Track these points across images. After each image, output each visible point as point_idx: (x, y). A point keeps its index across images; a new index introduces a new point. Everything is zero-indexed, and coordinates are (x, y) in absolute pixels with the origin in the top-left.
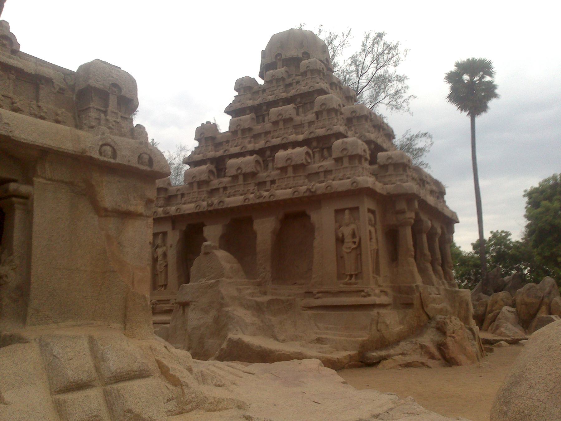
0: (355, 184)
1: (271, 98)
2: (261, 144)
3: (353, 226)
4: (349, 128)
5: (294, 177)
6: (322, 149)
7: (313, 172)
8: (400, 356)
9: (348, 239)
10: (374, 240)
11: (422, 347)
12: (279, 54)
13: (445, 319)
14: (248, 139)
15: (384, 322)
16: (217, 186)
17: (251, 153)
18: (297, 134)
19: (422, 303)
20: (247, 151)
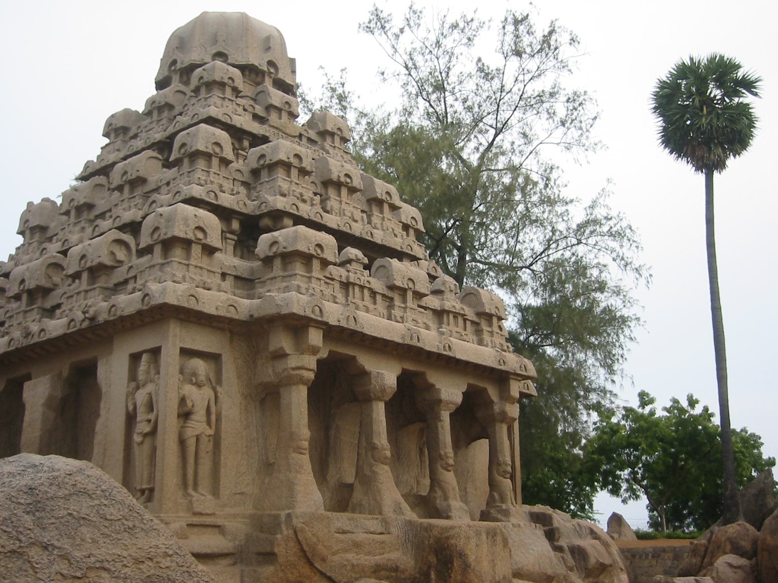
3: (150, 388)
7: (122, 280)
9: (141, 416)
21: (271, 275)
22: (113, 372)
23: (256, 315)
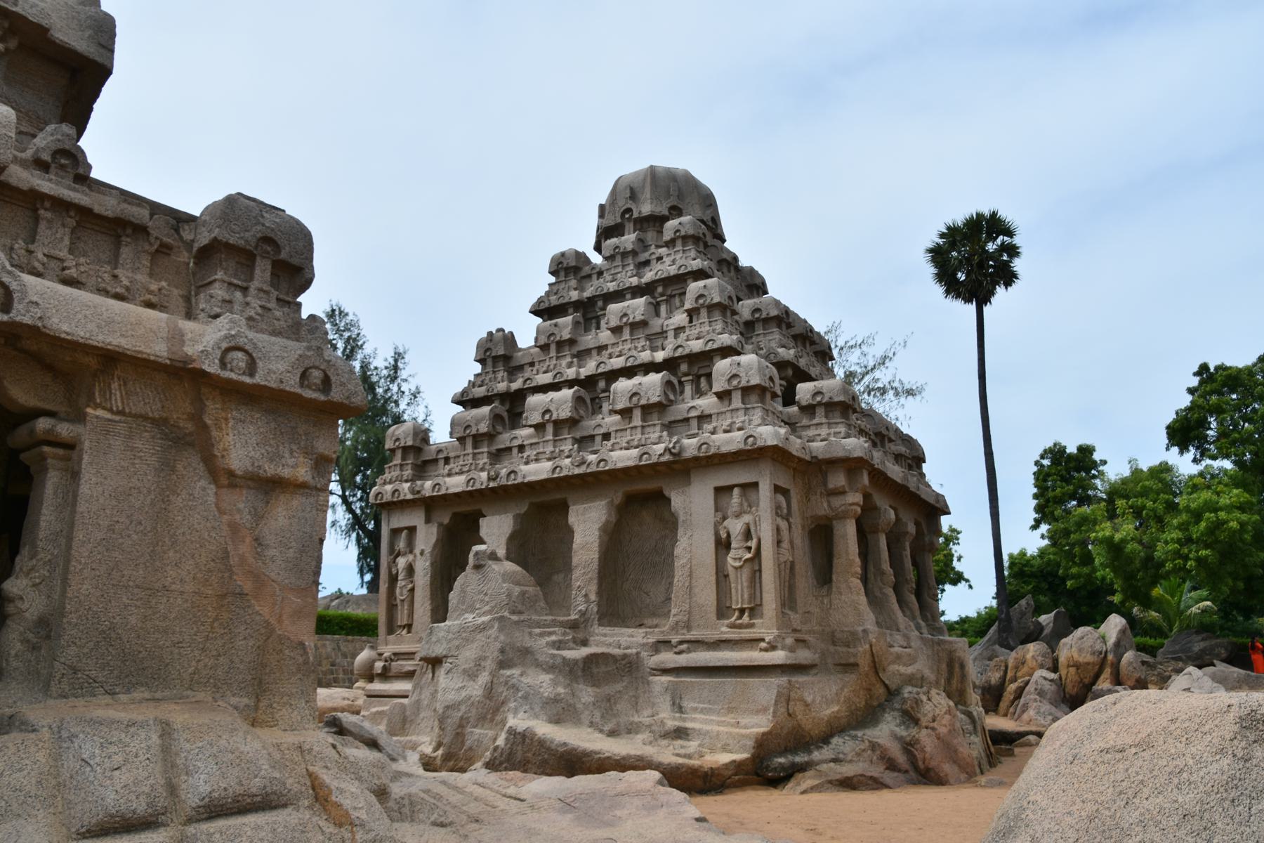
0: (751, 439)
1: (612, 286)
2: (590, 368)
3: (747, 518)
4: (748, 339)
5: (643, 427)
6: (698, 377)
7: (680, 418)
8: (832, 764)
10: (785, 544)
11: (874, 746)
12: (629, 210)
13: (918, 693)
14: (569, 359)
15: (802, 700)
16: (508, 444)
17: (570, 384)
18: (654, 349)
19: (874, 662)
20: (566, 381)
21: (815, 422)
22: (694, 503)
23: (820, 457)
